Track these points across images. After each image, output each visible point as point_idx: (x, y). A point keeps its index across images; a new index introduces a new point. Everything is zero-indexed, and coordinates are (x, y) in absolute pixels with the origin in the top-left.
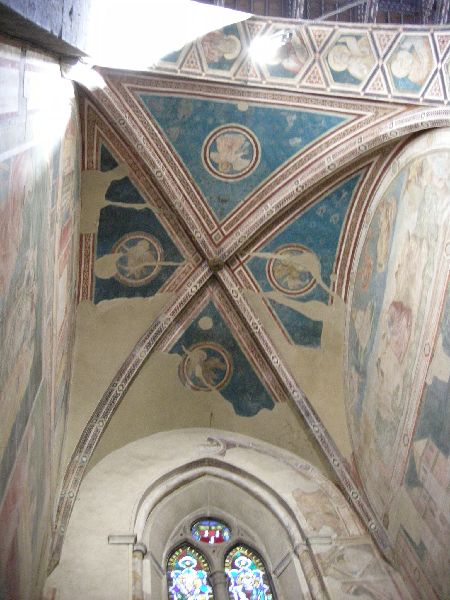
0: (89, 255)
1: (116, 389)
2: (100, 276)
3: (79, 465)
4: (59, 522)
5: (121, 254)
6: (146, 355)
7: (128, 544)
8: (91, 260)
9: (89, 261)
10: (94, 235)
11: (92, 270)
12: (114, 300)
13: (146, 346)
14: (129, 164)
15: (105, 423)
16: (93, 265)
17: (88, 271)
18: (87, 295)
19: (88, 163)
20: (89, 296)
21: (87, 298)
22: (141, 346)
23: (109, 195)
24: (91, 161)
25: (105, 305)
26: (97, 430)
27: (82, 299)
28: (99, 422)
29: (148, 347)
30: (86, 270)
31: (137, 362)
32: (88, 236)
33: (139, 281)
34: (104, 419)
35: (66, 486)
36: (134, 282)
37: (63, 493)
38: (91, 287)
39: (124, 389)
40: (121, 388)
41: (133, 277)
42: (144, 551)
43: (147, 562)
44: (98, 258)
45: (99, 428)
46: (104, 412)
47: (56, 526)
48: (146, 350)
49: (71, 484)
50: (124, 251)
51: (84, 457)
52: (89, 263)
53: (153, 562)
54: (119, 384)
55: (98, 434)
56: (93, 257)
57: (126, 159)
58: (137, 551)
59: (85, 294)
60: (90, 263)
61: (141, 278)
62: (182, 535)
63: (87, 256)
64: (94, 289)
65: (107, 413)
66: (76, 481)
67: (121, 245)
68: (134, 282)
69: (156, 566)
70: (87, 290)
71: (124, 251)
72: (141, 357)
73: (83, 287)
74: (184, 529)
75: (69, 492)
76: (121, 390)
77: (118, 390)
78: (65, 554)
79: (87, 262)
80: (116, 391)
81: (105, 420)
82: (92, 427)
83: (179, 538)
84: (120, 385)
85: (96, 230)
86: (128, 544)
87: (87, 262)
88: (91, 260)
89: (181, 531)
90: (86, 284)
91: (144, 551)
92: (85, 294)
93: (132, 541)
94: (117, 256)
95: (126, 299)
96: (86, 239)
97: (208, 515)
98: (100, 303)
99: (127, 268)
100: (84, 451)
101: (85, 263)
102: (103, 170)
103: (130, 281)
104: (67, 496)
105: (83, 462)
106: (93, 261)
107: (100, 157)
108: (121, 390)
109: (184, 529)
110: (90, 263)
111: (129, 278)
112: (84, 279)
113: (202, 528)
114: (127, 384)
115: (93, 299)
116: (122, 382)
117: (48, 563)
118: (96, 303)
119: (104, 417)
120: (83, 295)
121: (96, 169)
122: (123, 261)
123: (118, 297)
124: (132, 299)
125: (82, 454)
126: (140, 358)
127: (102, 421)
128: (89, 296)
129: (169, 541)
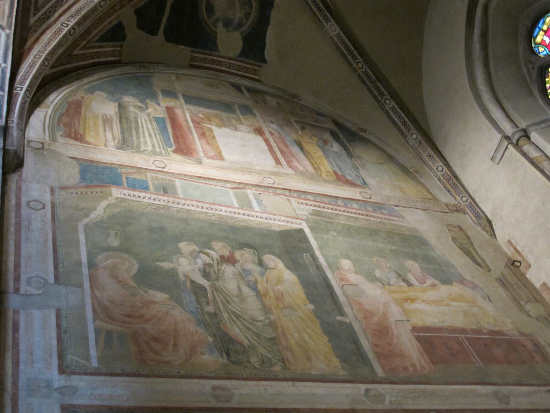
0: (213, 60)
1: (359, 71)
2: (238, 52)
3: (417, 145)
4: (457, 197)
5: (220, 25)
6: (335, 25)
7: (507, 148)
8: (219, 59)
9: (220, 61)
10: (192, 52)
11: (230, 59)
12: (267, 41)
13: (326, 22)
14: (121, 8)
15: (388, 97)
16: (224, 58)
17: (230, 64)
18: (255, 70)
19: (114, 56)
20: (256, 68)
21: (258, 71)
22: (324, 27)
23: (153, 32)
24: (113, 54)
25: (269, 53)
26: (392, 109)
27: (257, 76)
28: (385, 103)
29: (327, 20)
30: (228, 65)
31: (339, 37)
32: (192, 59)
33: (254, 9)
34: (384, 97)
35: (430, 168)
36: (252, 17)
37: (435, 175)
38: (247, 63)
39: (362, 62)
40: (360, 65)
41: (247, 16)
42: (523, 134)
43: (534, 136)
44: (218, 50)
45: (391, 106)
46: (378, 93)
47: (459, 202)
48: (329, 23)
49: (430, 163)
50: (217, 20)
51: (412, 136)
52: (222, 62)
53: (538, 127)
54: (355, 65)
55: (396, 109)
56: (216, 56)
57: (115, 11)
58: (517, 142)
59: (253, 72)
60: (222, 60)
61: (251, 7)
62: (533, 68)
63: (214, 62)
64: (250, 61)
65: (379, 90)
66: (430, 156)
67: (209, 23)
68: (252, 17)
69: (543, 125)
70: (249, 68)
71: (217, 20)
72: (335, 31)
73: (245, 72)
74: (530, 62)
75: (437, 169)
76: (363, 66)
77: (361, 70)
78: (487, 209)
79: (220, 64)
80: (362, 71)
81: (386, 96)
82: (387, 112)
83: (535, 73)
84: (357, 65)
85: (188, 49)
86: (507, 148)
87: (220, 64)
88: (219, 59)
89: (530, 66)
90: (242, 69)
91: (523, 134)
92: (253, 72)
93: (506, 143)
94: (220, 30)
95: (270, 28)
96: (195, 61)
97: (530, 24)
98: (266, 57)
99: (237, 20)
100: (406, 133)
101: (221, 65)
102: (124, 39)
103: (251, 20)
104: (439, 174)
105: (416, 139)
106: (220, 57)
107: (110, 43)
108: (363, 66)
109: (530, 62)
110: (222, 60)
111: (247, 20)
112: (238, 70)
113: (539, 39)
114: (359, 57)
115: (260, 64)
116: (355, 62)
117: (485, 233)
118: (265, 61)
119: (383, 96)
120: (254, 74)
121: (121, 46)
122: (228, 24)
123: (265, 36)
124: (272, 21)
125: (409, 136)
126: (336, 33)
127: (386, 99)
128: (256, 68)
129: (532, 87)
